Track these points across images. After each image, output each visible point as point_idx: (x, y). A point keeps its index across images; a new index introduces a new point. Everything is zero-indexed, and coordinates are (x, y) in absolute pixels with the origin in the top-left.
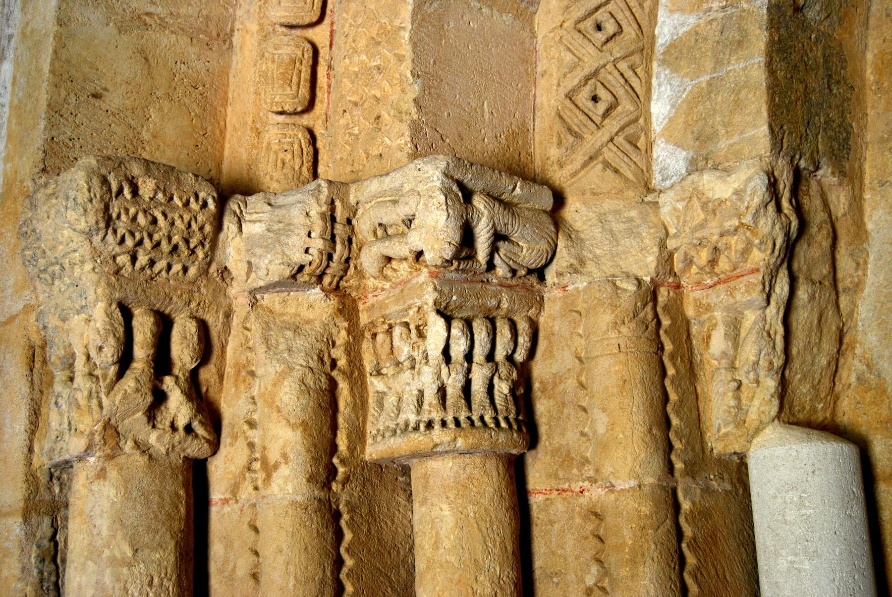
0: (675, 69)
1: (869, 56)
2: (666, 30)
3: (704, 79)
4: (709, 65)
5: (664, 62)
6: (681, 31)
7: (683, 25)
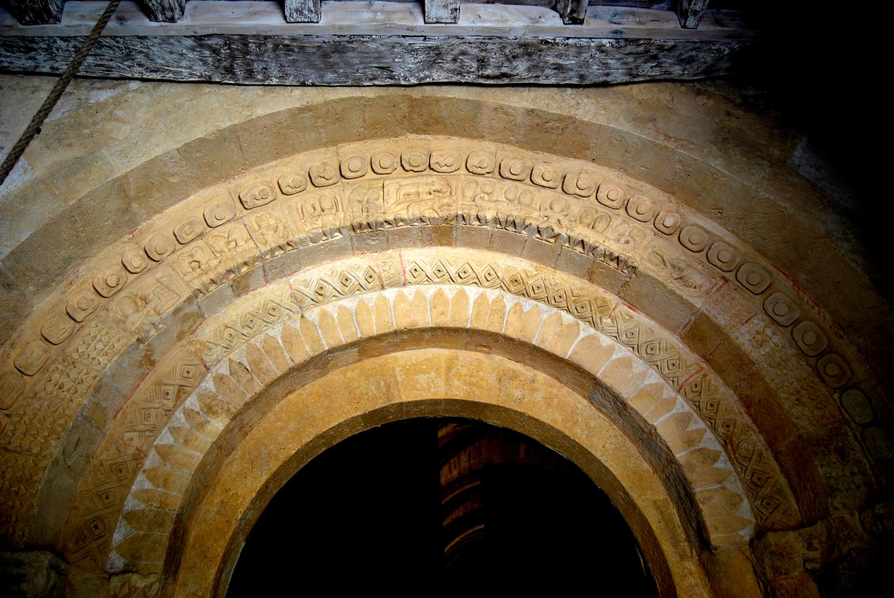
0: (130, 523)
1: (193, 533)
2: (130, 504)
3: (142, 533)
4: (145, 527)
5: (125, 518)
6: (137, 508)
7: (138, 506)
